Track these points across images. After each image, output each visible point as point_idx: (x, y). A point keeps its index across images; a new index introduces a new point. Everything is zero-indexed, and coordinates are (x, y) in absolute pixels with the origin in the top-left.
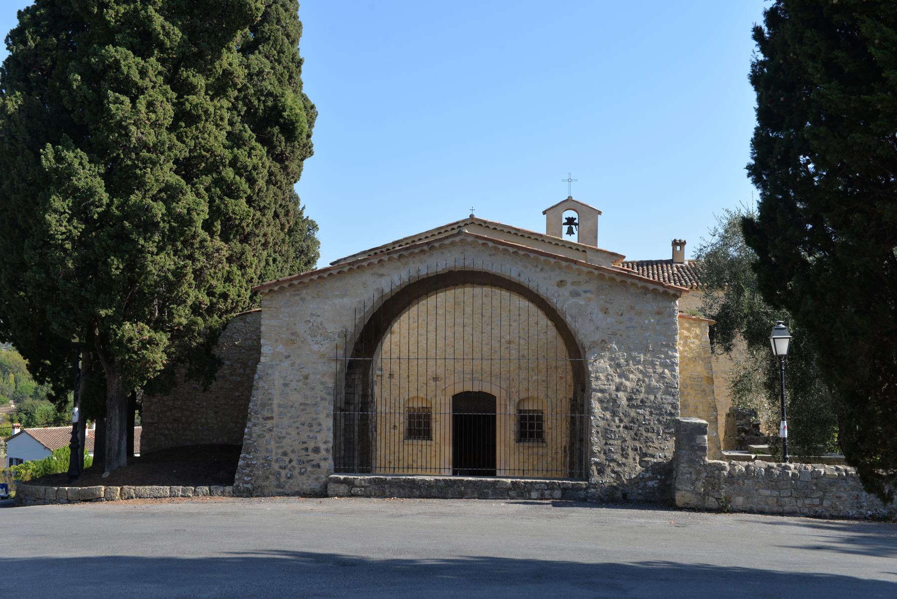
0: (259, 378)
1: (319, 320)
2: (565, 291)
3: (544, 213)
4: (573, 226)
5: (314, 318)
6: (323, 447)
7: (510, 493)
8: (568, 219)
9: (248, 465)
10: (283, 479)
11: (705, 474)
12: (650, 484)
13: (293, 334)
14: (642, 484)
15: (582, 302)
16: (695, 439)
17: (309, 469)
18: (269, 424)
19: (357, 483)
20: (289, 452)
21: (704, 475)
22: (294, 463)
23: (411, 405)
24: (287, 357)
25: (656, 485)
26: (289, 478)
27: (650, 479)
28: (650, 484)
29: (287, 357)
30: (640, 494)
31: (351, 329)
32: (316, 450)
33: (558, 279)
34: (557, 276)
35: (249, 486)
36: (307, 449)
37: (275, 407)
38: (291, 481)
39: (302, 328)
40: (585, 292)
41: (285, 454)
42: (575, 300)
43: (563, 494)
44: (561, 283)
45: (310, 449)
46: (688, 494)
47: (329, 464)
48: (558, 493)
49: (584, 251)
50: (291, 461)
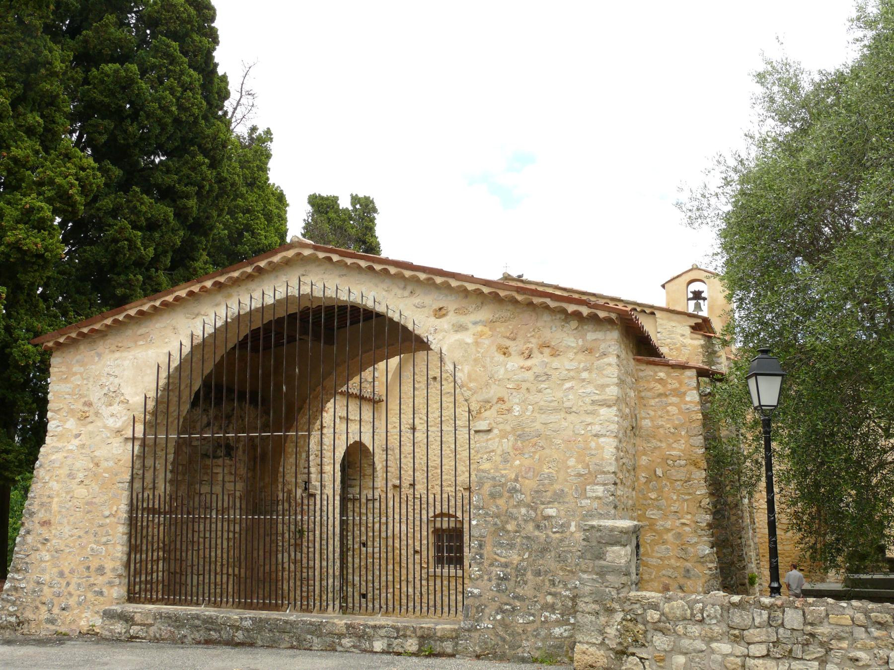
0: (41, 466)
1: (117, 381)
2: (444, 323)
3: (663, 286)
4: (701, 302)
5: (111, 379)
6: (109, 565)
7: (344, 641)
8: (694, 293)
9: (16, 589)
10: (56, 610)
11: (621, 615)
12: (557, 631)
13: (85, 404)
14: (543, 633)
15: (470, 340)
16: (604, 554)
17: (90, 595)
18: (45, 532)
19: (137, 618)
20: (66, 572)
21: (619, 616)
22: (71, 588)
23: (438, 525)
24: (77, 436)
25: (565, 634)
26: (64, 609)
27: (558, 623)
28: (557, 631)
29: (77, 436)
30: (538, 649)
31: (152, 394)
32: (101, 570)
33: (436, 306)
34: (432, 300)
35: (13, 619)
36: (88, 568)
37: (55, 507)
38: (65, 613)
39: (95, 395)
40: (475, 323)
41: (61, 574)
42: (459, 336)
43: (421, 645)
44: (440, 313)
45: (92, 569)
46: (592, 649)
47: (119, 591)
48: (412, 645)
49: (653, 313)
50: (68, 584)
